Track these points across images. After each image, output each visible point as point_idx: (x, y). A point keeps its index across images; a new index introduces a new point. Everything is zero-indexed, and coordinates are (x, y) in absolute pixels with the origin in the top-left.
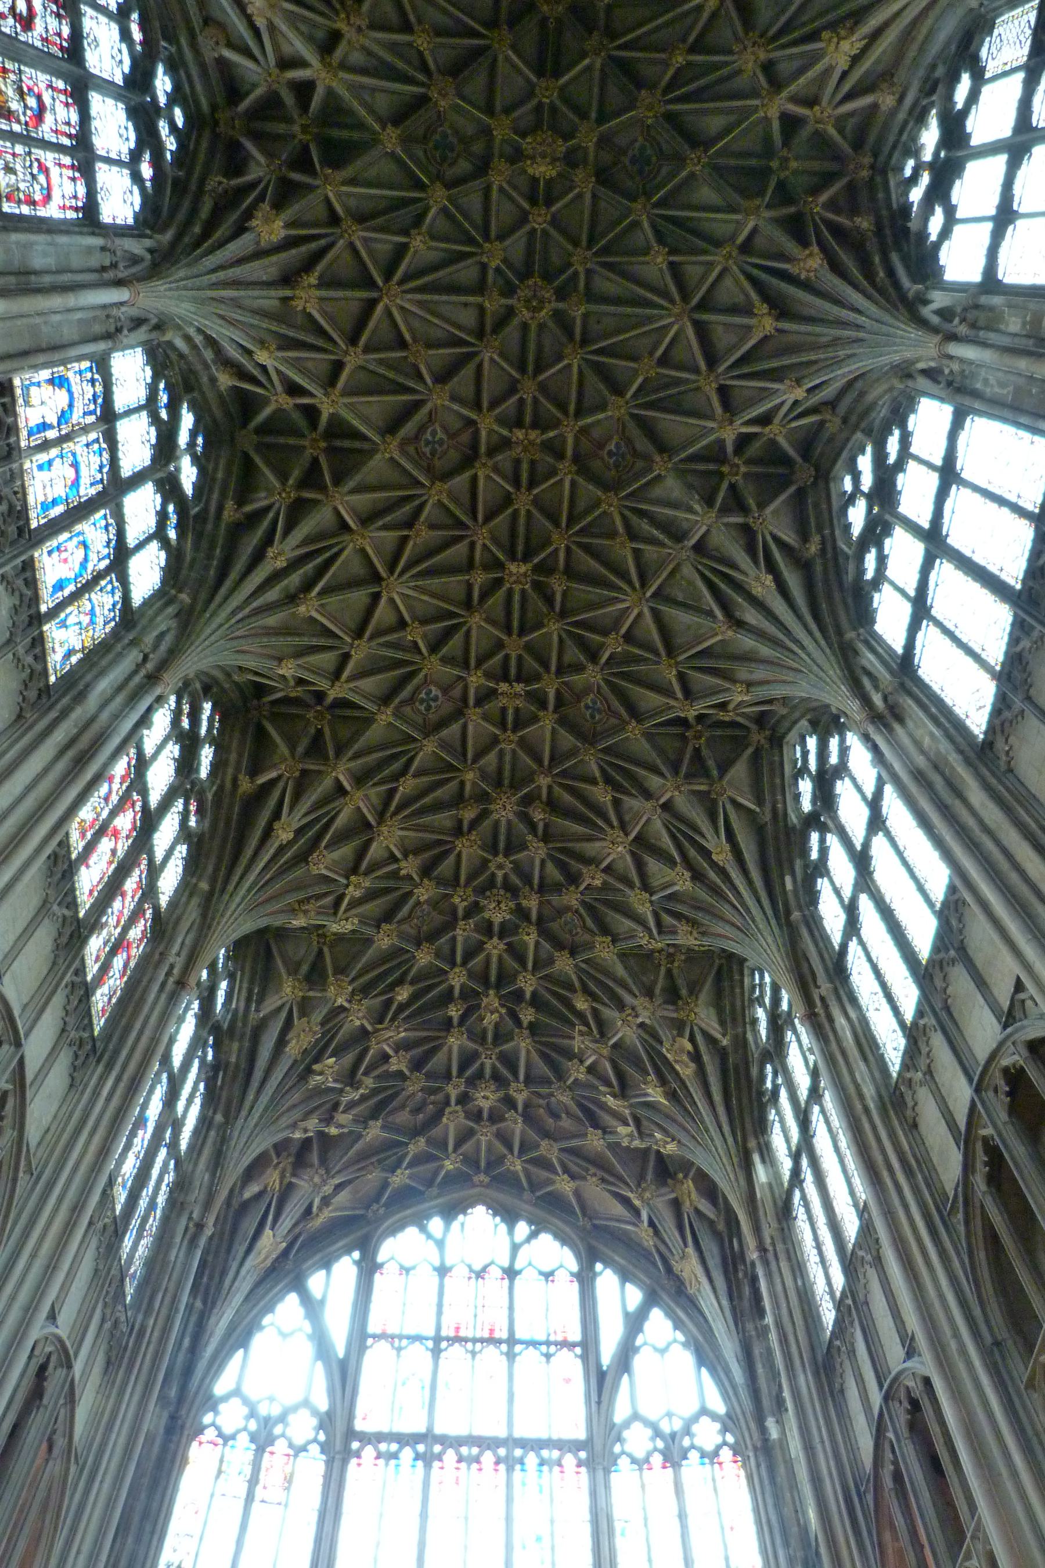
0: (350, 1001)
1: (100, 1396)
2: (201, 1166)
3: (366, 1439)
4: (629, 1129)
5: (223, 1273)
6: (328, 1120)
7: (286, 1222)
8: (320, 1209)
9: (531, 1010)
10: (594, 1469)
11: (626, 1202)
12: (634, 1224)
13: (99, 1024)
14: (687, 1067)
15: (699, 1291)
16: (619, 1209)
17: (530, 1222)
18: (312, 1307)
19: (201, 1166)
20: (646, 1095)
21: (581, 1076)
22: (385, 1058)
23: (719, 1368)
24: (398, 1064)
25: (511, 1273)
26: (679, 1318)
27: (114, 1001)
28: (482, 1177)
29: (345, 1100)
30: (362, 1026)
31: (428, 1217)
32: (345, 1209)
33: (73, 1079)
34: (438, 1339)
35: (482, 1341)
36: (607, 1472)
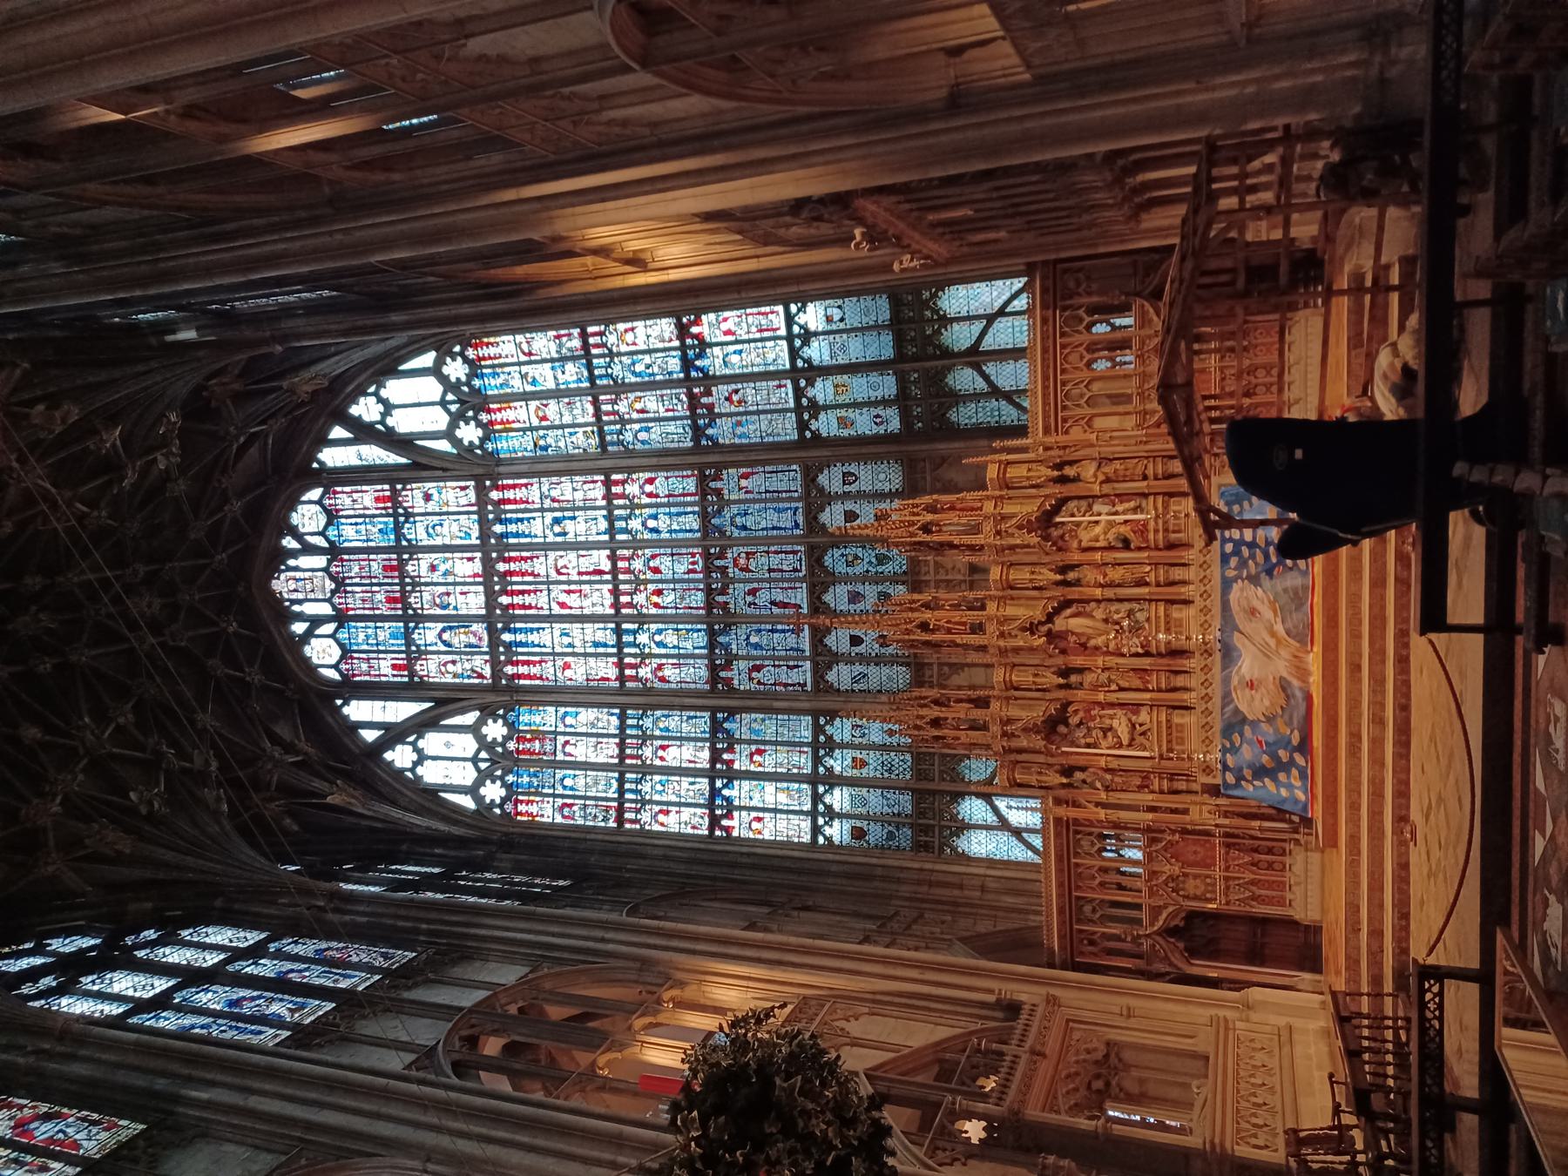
0: (55, 795)
1: (490, 958)
2: (272, 911)
3: (497, 673)
4: (159, 457)
5: (373, 830)
6: (202, 777)
7: (318, 784)
8: (297, 753)
9: (28, 580)
10: (499, 474)
11: (243, 449)
12: (267, 436)
13: (130, 1128)
14: (68, 412)
15: (324, 376)
16: (253, 451)
17: (282, 536)
18: (395, 734)
19: (272, 911)
20: (114, 445)
21: (104, 513)
22: (119, 729)
23: (396, 355)
24: (126, 717)
25: (334, 551)
26: (353, 390)
27: (95, 1116)
28: (240, 589)
29: (177, 764)
30: (83, 771)
31: (292, 635)
32: (296, 727)
33: (194, 1138)
34: (405, 618)
35: (402, 577)
36: (499, 462)
